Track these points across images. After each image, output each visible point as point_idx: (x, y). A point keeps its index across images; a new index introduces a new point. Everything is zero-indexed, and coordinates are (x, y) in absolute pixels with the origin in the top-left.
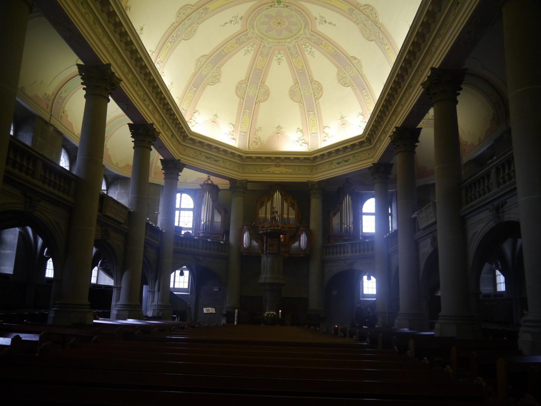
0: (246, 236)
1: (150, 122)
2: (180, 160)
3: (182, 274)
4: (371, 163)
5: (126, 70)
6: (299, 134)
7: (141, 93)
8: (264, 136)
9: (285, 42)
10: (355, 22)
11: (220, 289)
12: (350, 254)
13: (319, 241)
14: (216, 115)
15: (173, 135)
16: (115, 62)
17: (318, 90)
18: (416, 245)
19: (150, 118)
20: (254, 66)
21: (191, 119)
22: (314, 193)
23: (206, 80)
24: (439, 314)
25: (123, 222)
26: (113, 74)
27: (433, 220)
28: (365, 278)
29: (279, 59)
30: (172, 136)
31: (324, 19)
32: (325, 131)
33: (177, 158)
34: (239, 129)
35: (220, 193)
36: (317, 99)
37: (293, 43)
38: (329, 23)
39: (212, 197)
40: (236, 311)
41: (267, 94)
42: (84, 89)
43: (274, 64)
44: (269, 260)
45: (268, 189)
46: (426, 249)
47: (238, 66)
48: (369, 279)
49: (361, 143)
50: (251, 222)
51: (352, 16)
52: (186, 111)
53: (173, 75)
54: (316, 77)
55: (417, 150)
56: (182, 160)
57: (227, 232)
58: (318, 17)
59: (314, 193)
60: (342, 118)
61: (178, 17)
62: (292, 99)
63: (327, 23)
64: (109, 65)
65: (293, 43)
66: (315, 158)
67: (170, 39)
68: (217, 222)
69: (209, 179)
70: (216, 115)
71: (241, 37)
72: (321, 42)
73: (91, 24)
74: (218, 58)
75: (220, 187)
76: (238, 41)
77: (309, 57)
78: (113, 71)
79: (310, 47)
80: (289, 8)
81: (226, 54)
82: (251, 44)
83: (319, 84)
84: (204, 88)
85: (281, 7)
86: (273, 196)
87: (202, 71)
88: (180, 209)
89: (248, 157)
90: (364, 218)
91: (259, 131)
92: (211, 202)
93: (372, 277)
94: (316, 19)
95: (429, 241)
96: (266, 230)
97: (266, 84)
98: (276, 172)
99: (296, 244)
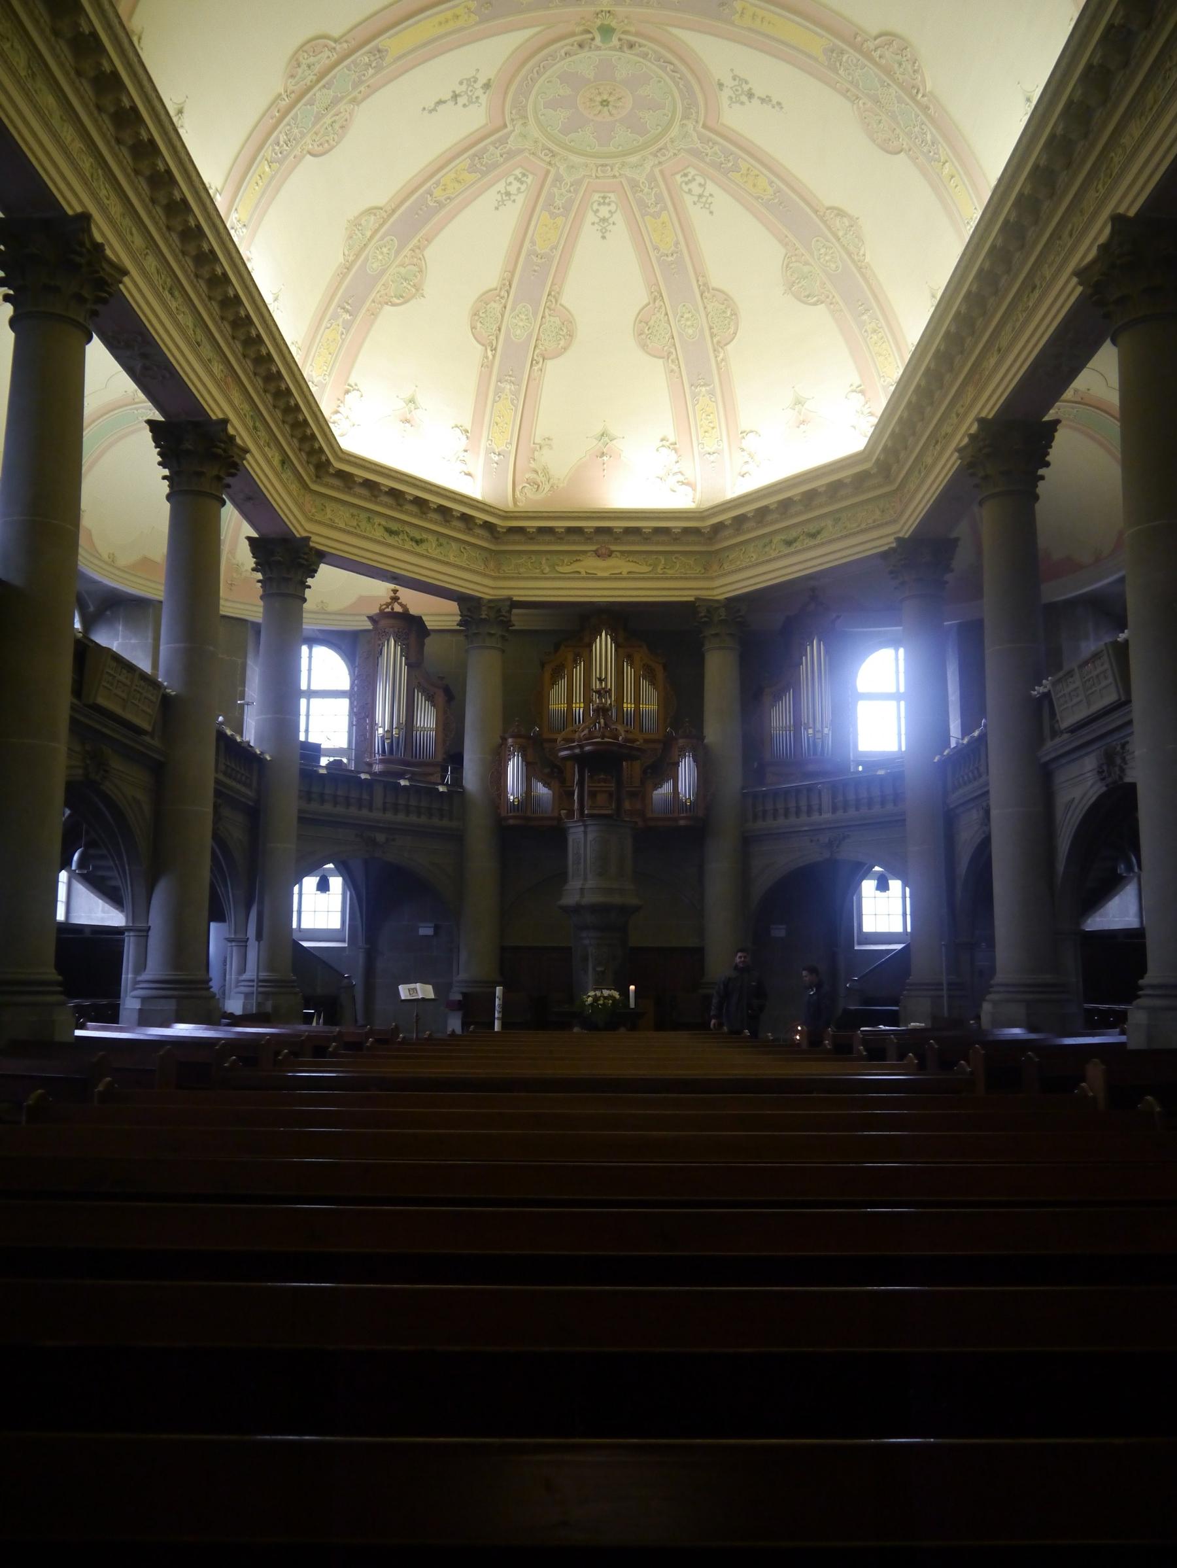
0: (513, 770)
1: (216, 414)
2: (308, 539)
3: (323, 886)
4: (891, 539)
5: (138, 241)
6: (668, 456)
7: (187, 320)
8: (559, 463)
9: (623, 165)
10: (845, 93)
11: (437, 928)
12: (827, 816)
13: (732, 779)
14: (412, 401)
15: (285, 461)
16: (104, 209)
17: (723, 316)
18: (1042, 781)
19: (217, 401)
20: (527, 244)
21: (337, 412)
22: (716, 635)
23: (379, 287)
24: (1141, 982)
25: (146, 726)
26: (99, 248)
27: (1111, 697)
28: (868, 886)
29: (604, 220)
30: (283, 463)
31: (746, 87)
32: (744, 444)
33: (299, 533)
34: (484, 443)
35: (427, 641)
36: (719, 346)
37: (648, 169)
38: (763, 100)
39: (406, 653)
40: (499, 990)
41: (567, 332)
42: (7, 298)
43: (589, 234)
44: (590, 837)
45: (577, 624)
46: (1080, 787)
47: (478, 241)
48: (883, 886)
49: (861, 480)
50: (525, 726)
51: (836, 72)
52: (323, 387)
53: (283, 259)
54: (717, 279)
55: (1041, 488)
56: (314, 538)
57: (456, 759)
58: (728, 82)
60: (799, 402)
61: (292, 76)
62: (644, 347)
63: (755, 101)
64: (85, 218)
65: (648, 166)
66: (718, 528)
67: (267, 152)
68: (424, 729)
69: (395, 599)
70: (412, 401)
71: (485, 150)
72: (734, 161)
73: (23, 73)
74: (413, 218)
75: (430, 623)
76: (477, 159)
77: (696, 214)
78: (99, 239)
79: (700, 179)
80: (637, 50)
81: (441, 205)
82: (518, 172)
83: (727, 299)
84: (374, 315)
85: (611, 49)
87: (367, 259)
89: (512, 530)
91: (545, 451)
92: (405, 669)
93: (895, 885)
94: (721, 85)
95: (1090, 762)
96: (581, 747)
97: (565, 300)
98: (600, 574)
99: (666, 789)
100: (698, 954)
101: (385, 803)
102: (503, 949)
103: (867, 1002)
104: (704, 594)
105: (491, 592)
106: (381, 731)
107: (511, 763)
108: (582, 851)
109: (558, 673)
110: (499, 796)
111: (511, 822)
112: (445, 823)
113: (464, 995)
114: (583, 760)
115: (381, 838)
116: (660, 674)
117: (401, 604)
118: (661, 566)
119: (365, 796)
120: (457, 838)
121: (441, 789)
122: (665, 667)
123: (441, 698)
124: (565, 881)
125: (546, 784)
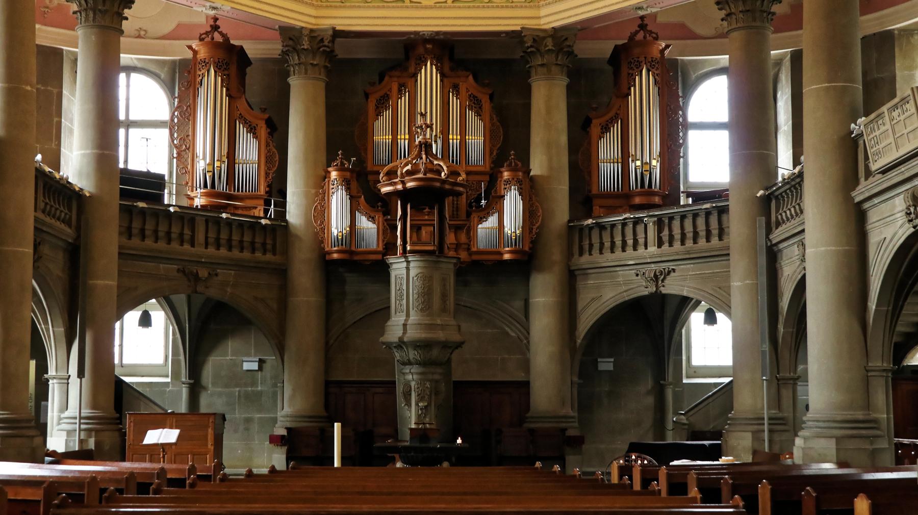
0: (338, 202)
3: (145, 321)
11: (261, 362)
13: (560, 210)
22: (542, 65)
28: (697, 318)
35: (248, 70)
39: (227, 83)
45: (400, 55)
48: (710, 318)
59: (542, 65)
68: (246, 163)
69: (215, 28)
86: (414, 76)
88: (129, 124)
90: (694, 138)
92: (226, 100)
96: (403, 183)
100: (524, 386)
101: (207, 238)
102: (328, 384)
103: (695, 435)
104: (531, 24)
105: (313, 21)
108: (405, 288)
109: (383, 103)
110: (323, 230)
111: (335, 256)
112: (269, 257)
113: (289, 430)
114: (405, 195)
115: (203, 273)
116: (486, 105)
117: (221, 33)
119: (187, 232)
120: (282, 273)
121: (263, 222)
122: (491, 97)
123: (263, 131)
124: (388, 317)
125: (371, 218)
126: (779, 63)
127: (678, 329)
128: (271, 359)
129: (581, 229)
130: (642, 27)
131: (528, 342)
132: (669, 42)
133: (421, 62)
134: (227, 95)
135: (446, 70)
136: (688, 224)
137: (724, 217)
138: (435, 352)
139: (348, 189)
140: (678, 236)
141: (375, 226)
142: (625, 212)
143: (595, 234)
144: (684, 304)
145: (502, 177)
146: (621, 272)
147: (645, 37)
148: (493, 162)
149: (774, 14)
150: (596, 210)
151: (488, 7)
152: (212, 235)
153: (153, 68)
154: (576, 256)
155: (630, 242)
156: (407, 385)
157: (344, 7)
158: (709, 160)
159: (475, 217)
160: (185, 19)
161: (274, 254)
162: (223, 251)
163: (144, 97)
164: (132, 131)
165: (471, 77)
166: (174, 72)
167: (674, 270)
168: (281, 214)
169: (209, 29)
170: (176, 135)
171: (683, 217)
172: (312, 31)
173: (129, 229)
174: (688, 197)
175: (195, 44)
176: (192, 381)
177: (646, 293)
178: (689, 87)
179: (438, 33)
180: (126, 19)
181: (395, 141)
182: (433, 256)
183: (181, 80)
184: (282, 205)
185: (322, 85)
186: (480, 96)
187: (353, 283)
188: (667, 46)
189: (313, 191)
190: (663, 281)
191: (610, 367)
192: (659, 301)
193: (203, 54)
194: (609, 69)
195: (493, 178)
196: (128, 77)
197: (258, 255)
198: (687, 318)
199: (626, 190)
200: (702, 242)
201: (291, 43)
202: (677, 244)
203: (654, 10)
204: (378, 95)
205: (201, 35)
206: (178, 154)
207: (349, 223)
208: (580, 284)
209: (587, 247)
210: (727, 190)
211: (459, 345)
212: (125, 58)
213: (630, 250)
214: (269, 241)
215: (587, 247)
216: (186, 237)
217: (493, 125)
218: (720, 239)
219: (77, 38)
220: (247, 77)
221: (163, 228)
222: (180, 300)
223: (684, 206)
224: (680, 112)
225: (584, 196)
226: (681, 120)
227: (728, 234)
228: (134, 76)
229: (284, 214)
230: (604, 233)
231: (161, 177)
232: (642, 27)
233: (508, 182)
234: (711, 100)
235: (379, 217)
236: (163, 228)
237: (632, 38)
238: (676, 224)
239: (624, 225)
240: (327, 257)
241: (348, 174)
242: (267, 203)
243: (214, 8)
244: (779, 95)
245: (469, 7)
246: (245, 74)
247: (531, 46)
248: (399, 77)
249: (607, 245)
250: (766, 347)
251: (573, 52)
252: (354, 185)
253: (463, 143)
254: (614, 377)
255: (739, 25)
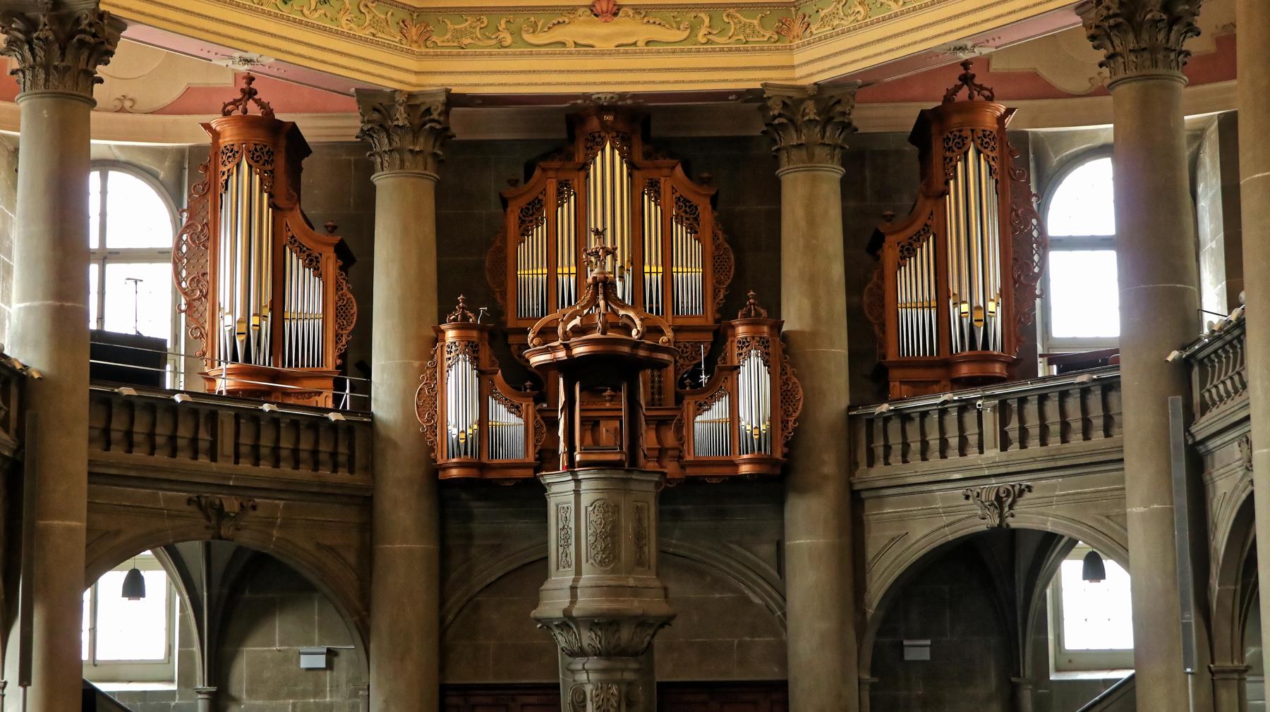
0: (458, 381)
3: (134, 587)
11: (331, 654)
13: (835, 391)
22: (800, 146)
28: (1071, 569)
35: (305, 162)
39: (270, 186)
45: (562, 133)
48: (1094, 570)
69: (250, 93)
86: (584, 167)
88: (108, 256)
92: (268, 213)
96: (568, 348)
98: (600, 46)
99: (719, 410)
101: (237, 445)
102: (444, 690)
105: (413, 79)
106: (228, 320)
107: (452, 373)
108: (572, 525)
109: (532, 214)
110: (433, 429)
111: (454, 473)
112: (343, 475)
114: (571, 368)
115: (231, 505)
116: (706, 214)
118: (704, 31)
119: (204, 435)
121: (333, 416)
122: (714, 201)
123: (331, 264)
124: (545, 575)
125: (515, 409)
126: (1198, 136)
127: (1037, 591)
128: (348, 649)
129: (870, 422)
130: (966, 79)
131: (784, 614)
132: (1012, 104)
133: (595, 144)
134: (269, 206)
135: (638, 157)
136: (1052, 408)
137: (1113, 397)
138: (625, 634)
139: (475, 360)
140: (1034, 431)
141: (521, 421)
142: (944, 391)
143: (894, 426)
144: (1049, 547)
145: (734, 335)
146: (941, 495)
147: (971, 97)
148: (718, 311)
149: (1188, 53)
150: (896, 388)
151: (706, 51)
152: (246, 440)
153: (146, 162)
154: (863, 465)
155: (954, 441)
156: (579, 692)
157: (465, 55)
158: (1085, 301)
159: (689, 404)
160: (198, 81)
161: (351, 471)
162: (265, 468)
163: (129, 211)
164: (111, 268)
165: (679, 171)
166: (181, 169)
167: (1029, 488)
168: (363, 405)
169: (239, 96)
170: (184, 273)
171: (1043, 399)
172: (411, 95)
173: (106, 431)
174: (1050, 363)
175: (216, 121)
176: (213, 689)
177: (984, 528)
178: (1048, 180)
179: (622, 96)
180: (101, 81)
181: (552, 277)
182: (620, 469)
183: (191, 183)
184: (364, 387)
185: (428, 187)
186: (695, 200)
187: (485, 519)
188: (1009, 111)
189: (416, 364)
190: (1011, 507)
191: (925, 655)
192: (1006, 538)
193: (229, 136)
194: (912, 150)
195: (720, 336)
196: (104, 178)
197: (325, 472)
198: (1055, 568)
199: (945, 354)
200: (1076, 440)
201: (376, 116)
202: (1034, 445)
203: (985, 51)
204: (523, 202)
205: (226, 106)
206: (189, 304)
207: (477, 417)
208: (872, 514)
209: (880, 451)
210: (1117, 351)
211: (666, 621)
212: (99, 146)
213: (953, 456)
214: (343, 449)
215: (880, 451)
216: (203, 445)
217: (718, 247)
218: (1108, 434)
219: (18, 113)
220: (303, 175)
221: (162, 430)
222: (193, 550)
223: (1044, 379)
224: (1034, 221)
225: (874, 366)
226: (1035, 233)
227: (1121, 427)
228: (114, 175)
229: (367, 403)
230: (908, 427)
231: (161, 344)
232: (966, 79)
233: (743, 343)
234: (1085, 199)
235: (528, 405)
236: (162, 430)
237: (948, 99)
238: (1032, 408)
239: (943, 412)
240: (441, 476)
241: (475, 334)
242: (339, 385)
243: (247, 61)
244: (1200, 189)
245: (674, 52)
246: (301, 169)
247: (780, 115)
248: (557, 170)
249: (915, 446)
250: (1192, 617)
251: (850, 124)
252: (485, 353)
253: (668, 278)
254: (929, 671)
255: (1129, 74)
